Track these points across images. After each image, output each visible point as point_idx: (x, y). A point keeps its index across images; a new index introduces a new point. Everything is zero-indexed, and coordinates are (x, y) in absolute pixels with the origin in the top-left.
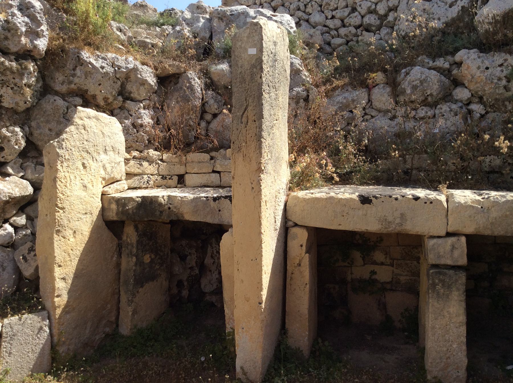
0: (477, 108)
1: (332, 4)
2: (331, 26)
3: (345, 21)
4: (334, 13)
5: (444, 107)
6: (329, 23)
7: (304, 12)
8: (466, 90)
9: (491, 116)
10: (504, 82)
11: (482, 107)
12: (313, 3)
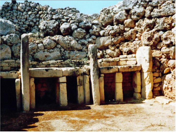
0: (62, 50)
1: (20, 17)
2: (20, 24)
3: (24, 23)
4: (21, 20)
5: (56, 49)
6: (19, 23)
7: (11, 19)
8: (60, 46)
9: (66, 51)
10: (68, 44)
11: (63, 49)
12: (14, 16)
